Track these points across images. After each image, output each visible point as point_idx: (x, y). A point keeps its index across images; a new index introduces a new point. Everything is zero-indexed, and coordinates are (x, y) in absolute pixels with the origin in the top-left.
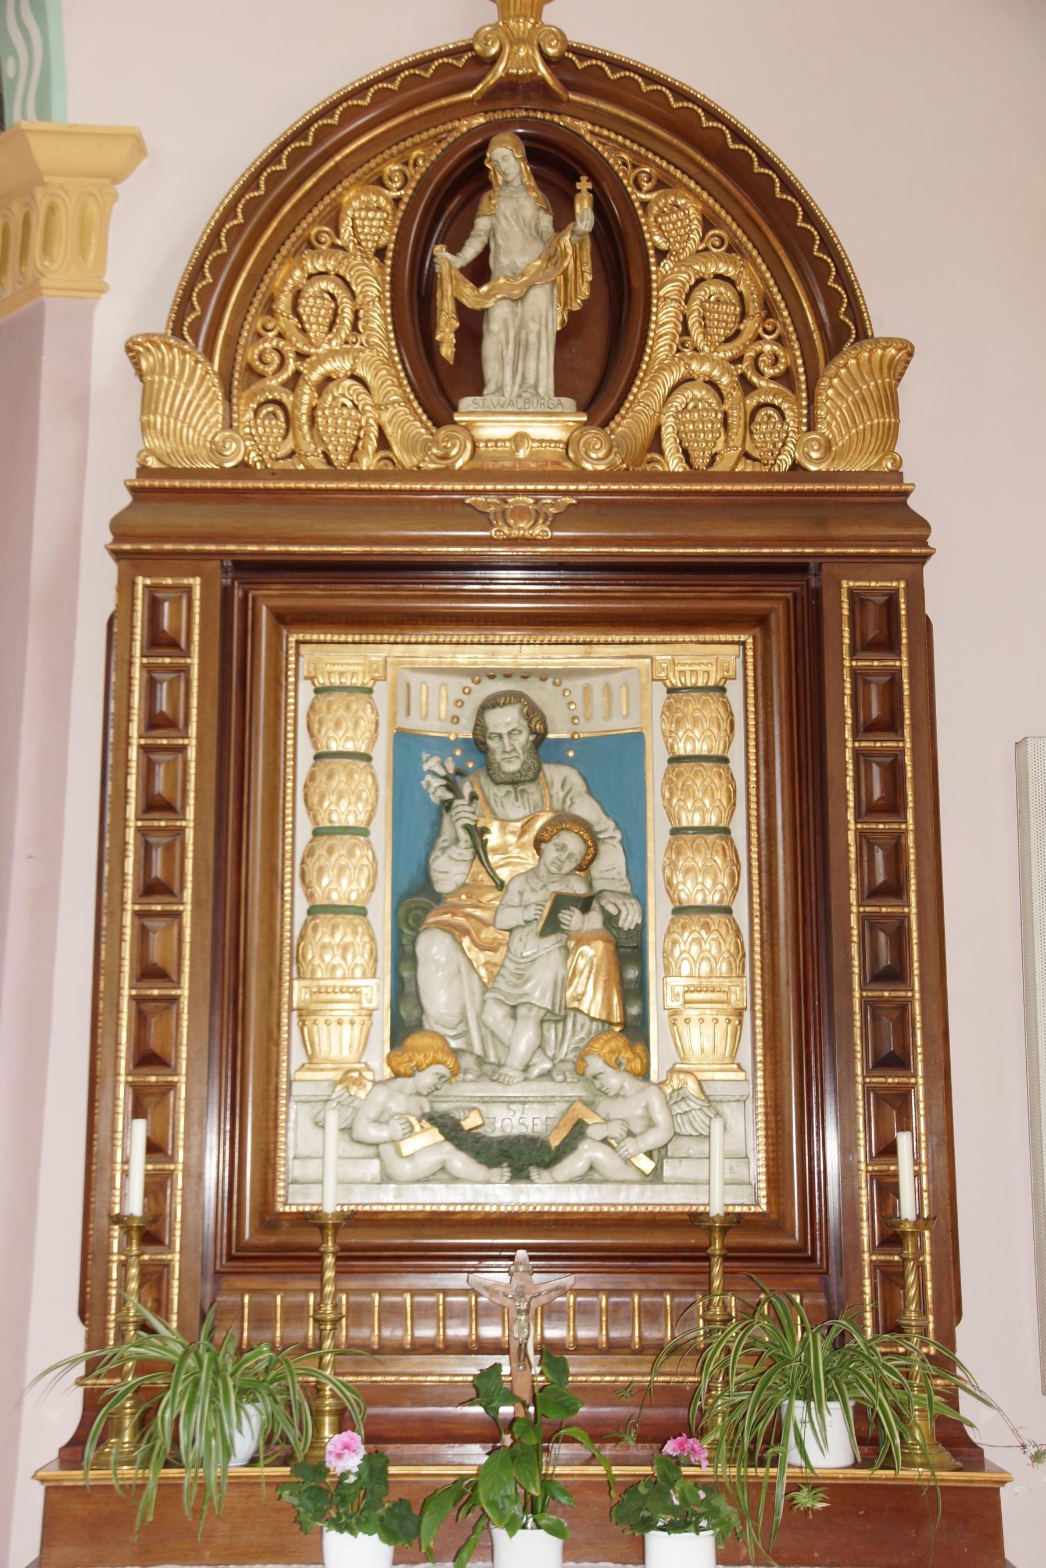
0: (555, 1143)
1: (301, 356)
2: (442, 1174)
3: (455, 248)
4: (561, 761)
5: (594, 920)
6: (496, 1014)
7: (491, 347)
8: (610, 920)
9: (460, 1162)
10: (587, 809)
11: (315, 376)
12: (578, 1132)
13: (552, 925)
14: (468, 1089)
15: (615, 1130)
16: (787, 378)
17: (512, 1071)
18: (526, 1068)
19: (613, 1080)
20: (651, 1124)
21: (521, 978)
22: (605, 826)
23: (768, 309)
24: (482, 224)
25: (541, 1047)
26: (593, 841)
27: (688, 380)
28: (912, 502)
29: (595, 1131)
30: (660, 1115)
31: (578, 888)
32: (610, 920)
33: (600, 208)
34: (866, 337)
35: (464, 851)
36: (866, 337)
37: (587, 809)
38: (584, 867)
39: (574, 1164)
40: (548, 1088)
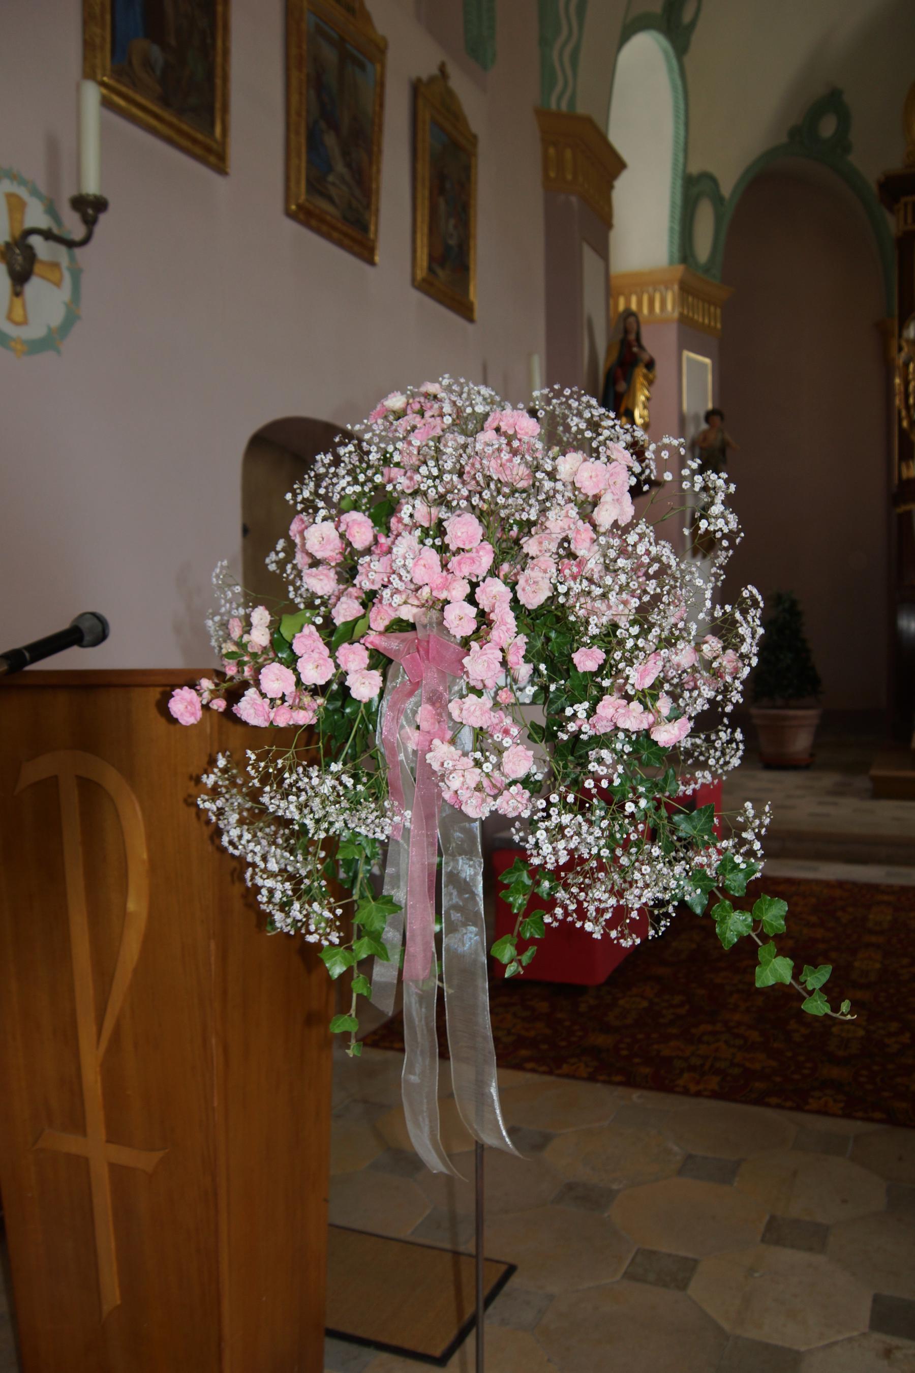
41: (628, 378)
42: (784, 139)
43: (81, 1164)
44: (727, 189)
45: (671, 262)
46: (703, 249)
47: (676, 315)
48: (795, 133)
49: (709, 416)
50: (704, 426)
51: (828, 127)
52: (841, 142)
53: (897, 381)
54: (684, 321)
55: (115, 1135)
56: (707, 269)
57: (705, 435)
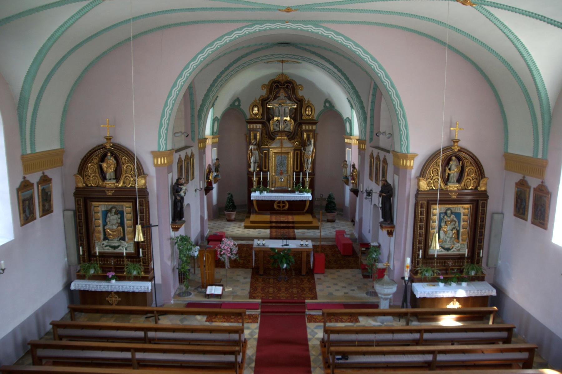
0: (451, 248)
1: (433, 177)
2: (442, 251)
3: (448, 167)
4: (453, 214)
5: (455, 229)
6: (446, 237)
7: (450, 177)
8: (457, 229)
9: (443, 250)
10: (455, 219)
11: (434, 178)
12: (453, 248)
13: (452, 230)
14: (444, 244)
15: (456, 247)
16: (477, 179)
17: (447, 242)
18: (449, 242)
19: (456, 243)
20: (459, 247)
21: (449, 234)
22: (457, 220)
23: (476, 172)
24: (450, 165)
25: (450, 240)
26: (455, 222)
27: (468, 179)
28: (488, 194)
29: (454, 247)
30: (460, 246)
31: (454, 226)
32: (457, 229)
33: (462, 163)
34: (485, 177)
35: (444, 223)
36: (485, 177)
37: (455, 219)
38: (454, 225)
39: (452, 250)
40: (450, 244)
41: (210, 174)
42: (229, 106)
43: (206, 273)
44: (219, 118)
45: (210, 135)
46: (215, 130)
47: (211, 143)
48: (231, 105)
49: (217, 159)
50: (215, 161)
51: (237, 103)
52: (239, 105)
53: (248, 155)
54: (213, 143)
55: (208, 270)
56: (216, 133)
57: (216, 162)
